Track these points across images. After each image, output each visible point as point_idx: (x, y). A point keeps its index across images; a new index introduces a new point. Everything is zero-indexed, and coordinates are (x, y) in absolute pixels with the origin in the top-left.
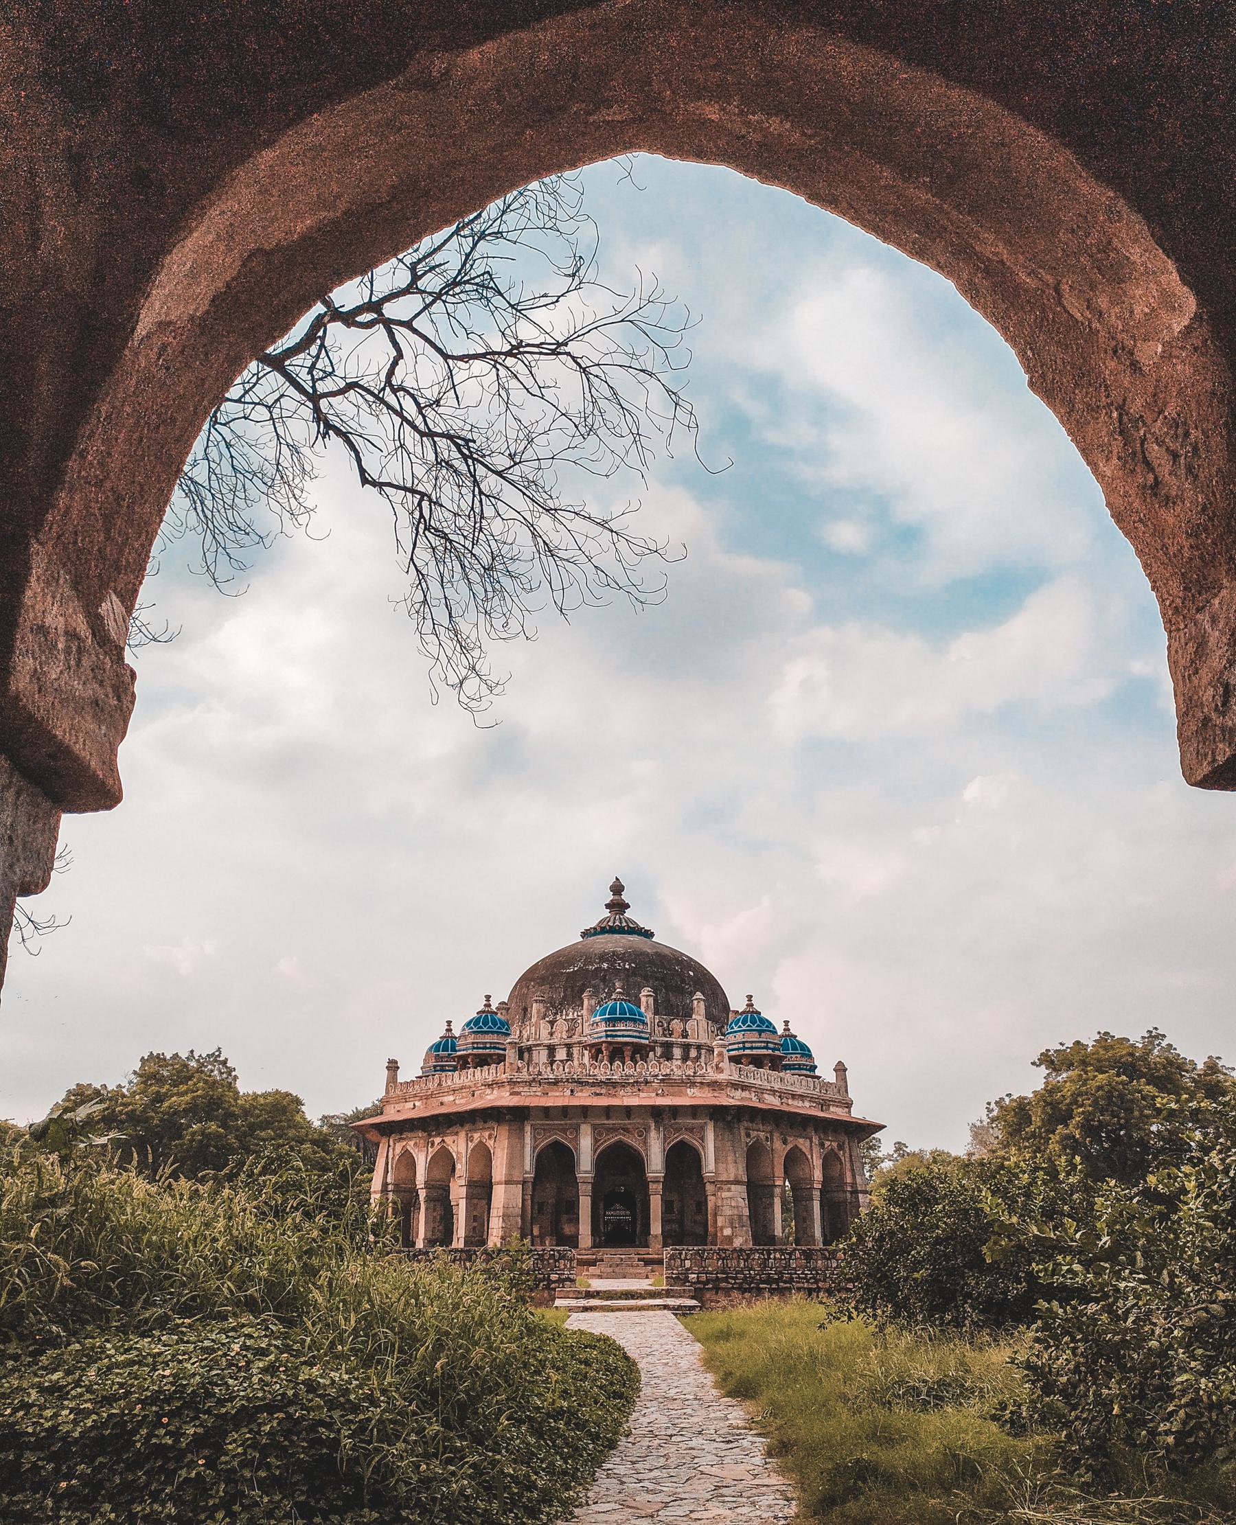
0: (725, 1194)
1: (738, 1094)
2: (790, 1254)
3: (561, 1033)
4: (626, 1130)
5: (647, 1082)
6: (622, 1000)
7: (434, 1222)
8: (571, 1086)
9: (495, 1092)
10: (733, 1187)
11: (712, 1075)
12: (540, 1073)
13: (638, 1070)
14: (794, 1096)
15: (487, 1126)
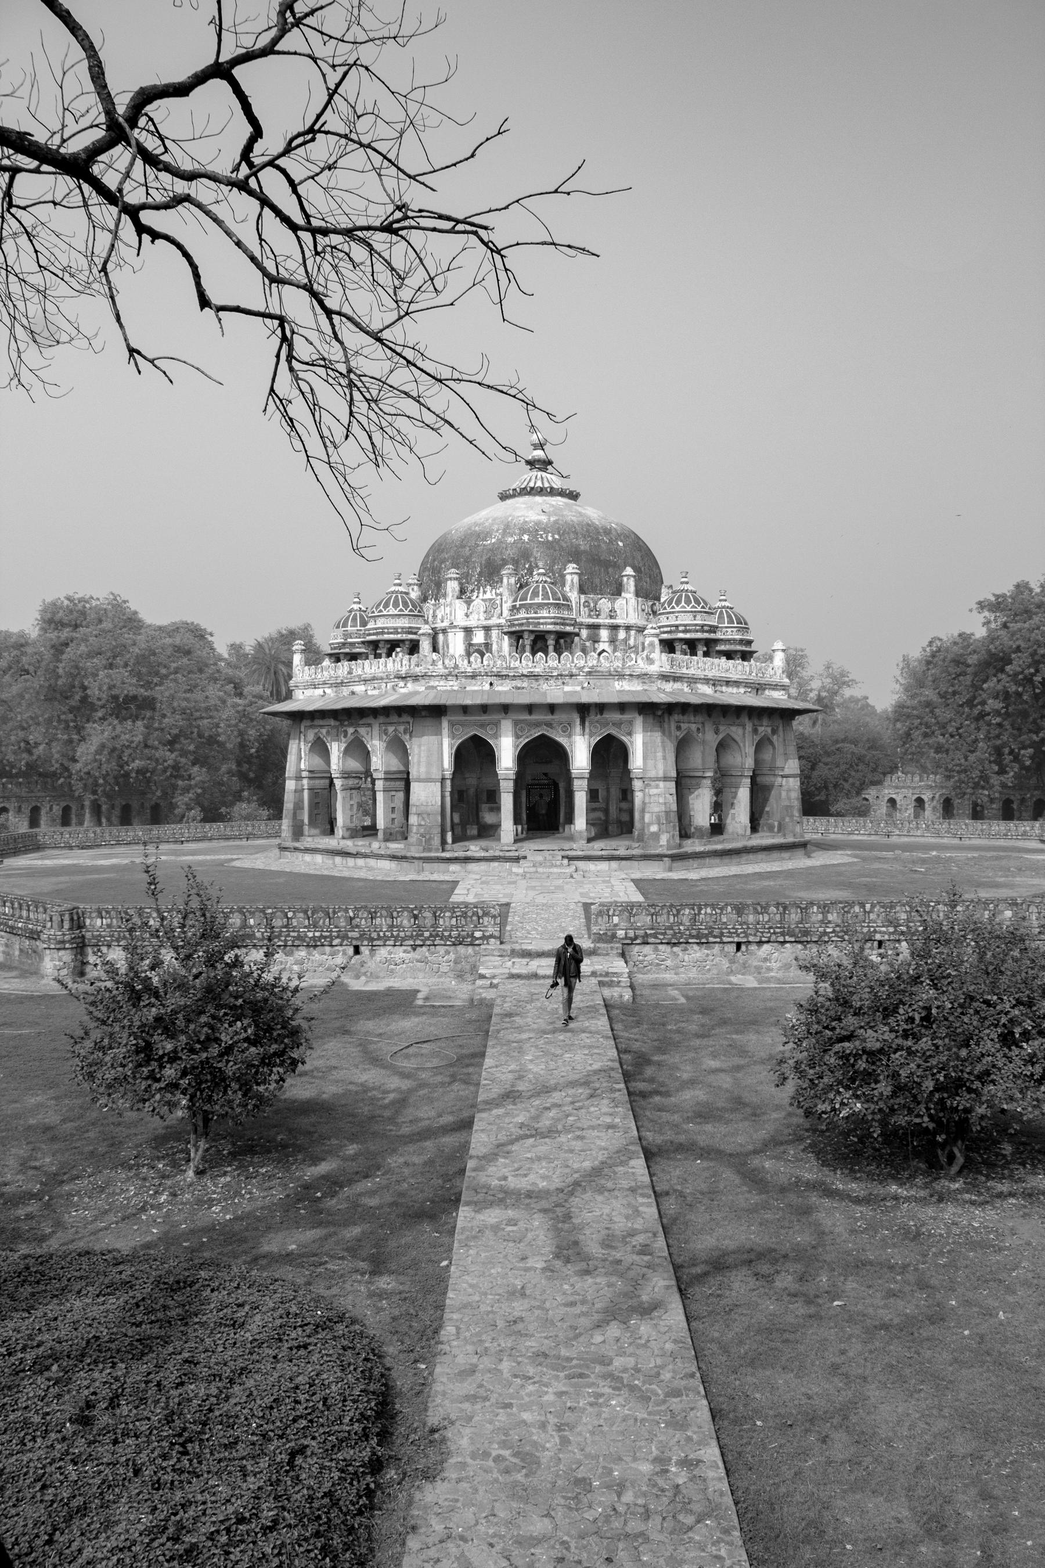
0: (653, 791)
1: (669, 687)
2: (721, 909)
3: (479, 613)
4: (549, 725)
5: (571, 676)
6: (546, 582)
7: (351, 809)
8: (489, 680)
9: (409, 685)
10: (661, 784)
11: (642, 666)
12: (456, 666)
13: (563, 662)
14: (728, 683)
15: (402, 720)
